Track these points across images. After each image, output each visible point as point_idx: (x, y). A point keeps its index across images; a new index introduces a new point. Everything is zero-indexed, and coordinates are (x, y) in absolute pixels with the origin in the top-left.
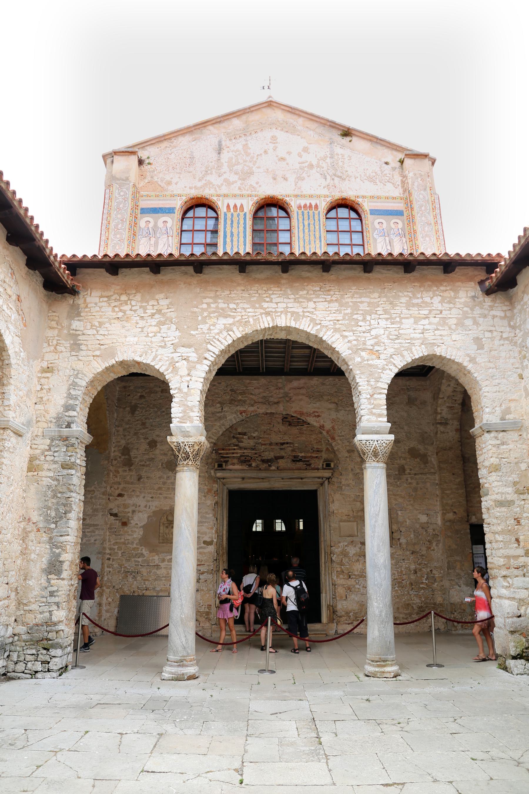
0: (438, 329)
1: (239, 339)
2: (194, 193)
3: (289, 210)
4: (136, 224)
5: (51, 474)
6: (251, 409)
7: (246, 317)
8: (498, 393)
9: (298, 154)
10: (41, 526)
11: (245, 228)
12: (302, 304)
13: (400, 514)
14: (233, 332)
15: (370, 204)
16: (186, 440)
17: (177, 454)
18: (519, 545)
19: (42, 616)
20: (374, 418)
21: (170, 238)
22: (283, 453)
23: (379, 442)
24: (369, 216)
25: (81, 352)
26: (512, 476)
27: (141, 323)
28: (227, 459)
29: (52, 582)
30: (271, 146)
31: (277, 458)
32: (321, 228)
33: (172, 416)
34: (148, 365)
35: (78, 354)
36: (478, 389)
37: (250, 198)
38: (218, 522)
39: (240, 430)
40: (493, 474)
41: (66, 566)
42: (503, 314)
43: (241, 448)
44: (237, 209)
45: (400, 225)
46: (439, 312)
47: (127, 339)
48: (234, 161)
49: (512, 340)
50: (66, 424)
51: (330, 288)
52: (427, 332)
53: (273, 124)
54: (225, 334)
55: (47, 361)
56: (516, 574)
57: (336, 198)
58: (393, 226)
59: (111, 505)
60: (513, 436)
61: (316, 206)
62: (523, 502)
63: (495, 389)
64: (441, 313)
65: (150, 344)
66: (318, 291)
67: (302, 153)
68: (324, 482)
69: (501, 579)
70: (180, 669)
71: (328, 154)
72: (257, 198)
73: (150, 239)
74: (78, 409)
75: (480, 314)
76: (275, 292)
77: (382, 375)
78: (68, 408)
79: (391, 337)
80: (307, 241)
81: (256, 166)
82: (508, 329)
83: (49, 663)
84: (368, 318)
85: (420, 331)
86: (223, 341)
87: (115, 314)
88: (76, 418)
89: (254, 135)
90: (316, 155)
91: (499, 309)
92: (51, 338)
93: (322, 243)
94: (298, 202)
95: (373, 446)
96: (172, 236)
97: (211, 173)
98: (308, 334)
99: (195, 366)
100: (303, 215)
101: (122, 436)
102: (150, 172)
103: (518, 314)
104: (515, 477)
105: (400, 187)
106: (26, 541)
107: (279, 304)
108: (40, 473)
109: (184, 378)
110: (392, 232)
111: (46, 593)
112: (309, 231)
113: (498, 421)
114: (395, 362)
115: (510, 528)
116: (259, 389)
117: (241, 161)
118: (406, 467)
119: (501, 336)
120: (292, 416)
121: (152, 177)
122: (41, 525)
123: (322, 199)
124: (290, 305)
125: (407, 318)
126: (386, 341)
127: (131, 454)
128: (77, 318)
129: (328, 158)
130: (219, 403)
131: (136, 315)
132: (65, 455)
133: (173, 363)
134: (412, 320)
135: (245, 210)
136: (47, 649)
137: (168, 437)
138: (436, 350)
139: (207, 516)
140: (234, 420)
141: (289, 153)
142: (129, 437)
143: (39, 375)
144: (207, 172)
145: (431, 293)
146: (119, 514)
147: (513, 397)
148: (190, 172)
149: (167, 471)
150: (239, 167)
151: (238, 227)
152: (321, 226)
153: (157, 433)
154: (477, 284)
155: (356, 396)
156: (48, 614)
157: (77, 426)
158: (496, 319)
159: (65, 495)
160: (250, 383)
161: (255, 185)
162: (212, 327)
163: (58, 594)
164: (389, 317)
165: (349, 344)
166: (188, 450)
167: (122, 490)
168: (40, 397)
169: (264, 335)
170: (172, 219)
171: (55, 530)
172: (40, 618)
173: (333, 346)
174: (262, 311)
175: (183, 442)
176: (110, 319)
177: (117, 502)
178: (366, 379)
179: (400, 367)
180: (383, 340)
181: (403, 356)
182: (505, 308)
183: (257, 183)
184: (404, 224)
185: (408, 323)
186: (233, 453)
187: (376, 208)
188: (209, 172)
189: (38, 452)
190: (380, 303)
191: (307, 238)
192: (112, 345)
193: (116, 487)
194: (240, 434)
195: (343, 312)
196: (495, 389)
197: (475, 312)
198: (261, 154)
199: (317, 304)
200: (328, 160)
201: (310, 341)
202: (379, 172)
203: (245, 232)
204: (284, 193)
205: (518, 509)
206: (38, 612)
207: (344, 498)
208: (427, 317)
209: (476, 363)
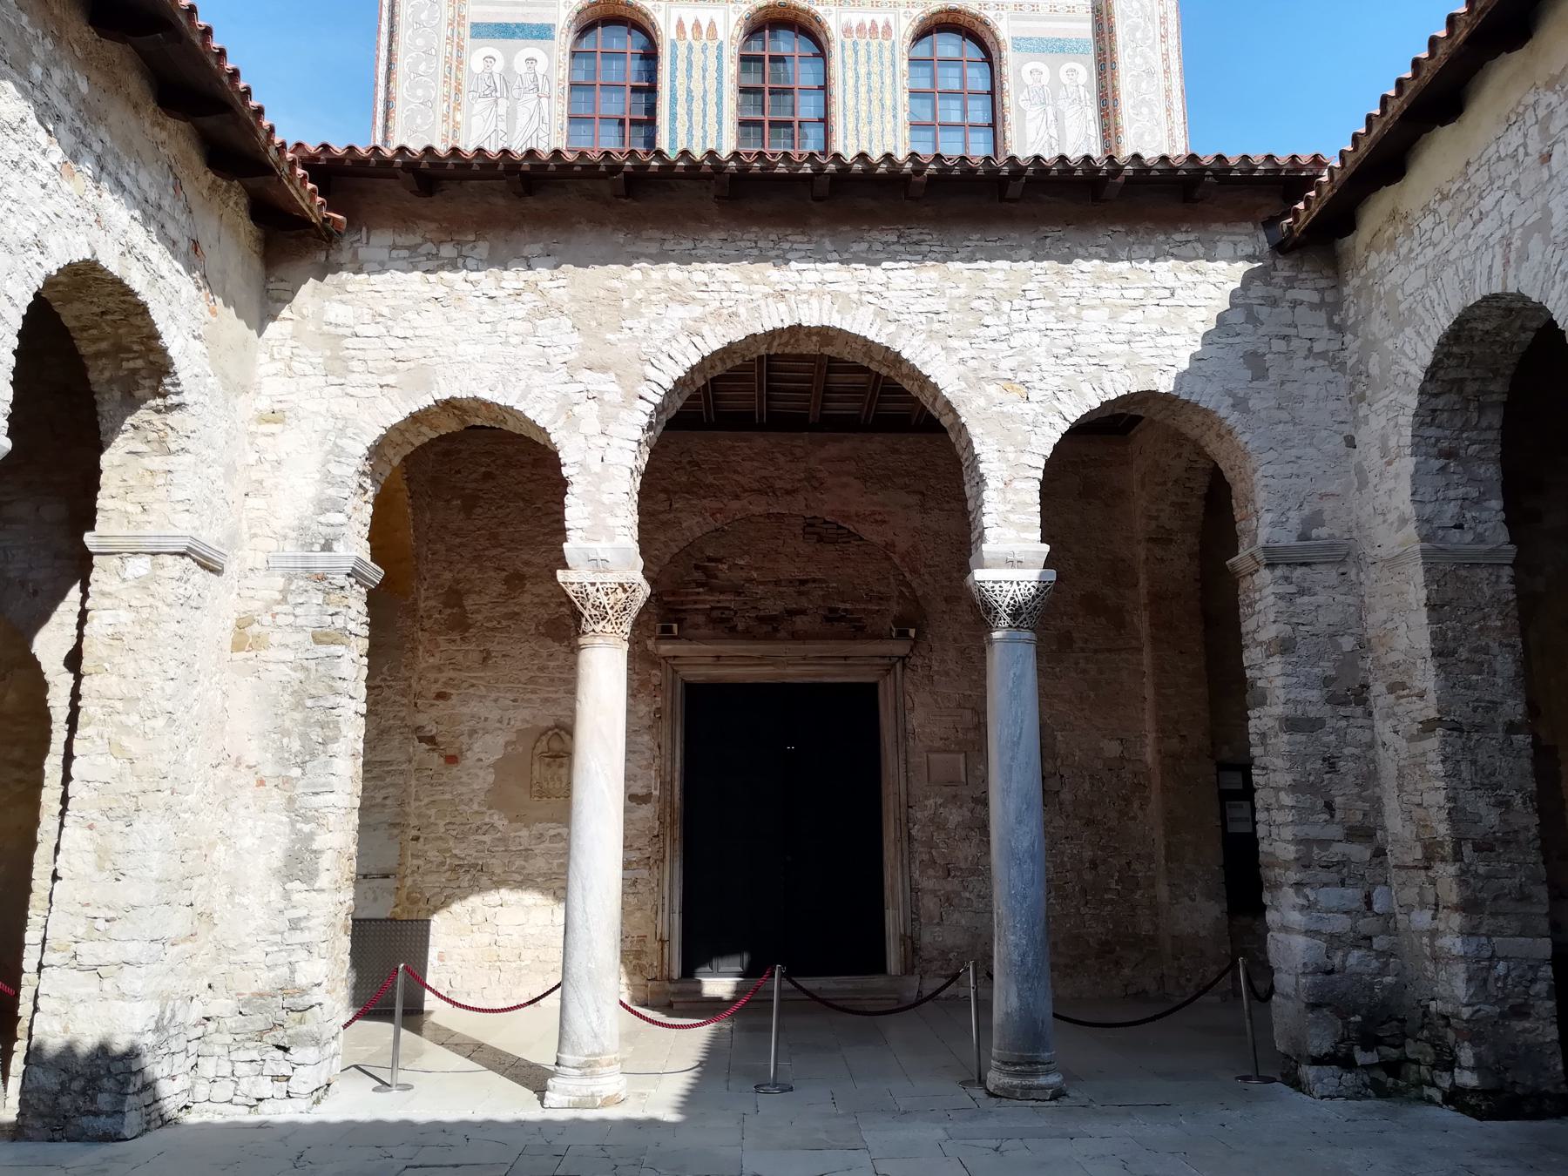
0: (1164, 333)
1: (714, 353)
3: (822, 38)
4: (462, 63)
5: (289, 655)
6: (735, 505)
7: (732, 303)
8: (1294, 480)
10: (268, 774)
11: (720, 82)
12: (856, 273)
13: (1060, 738)
14: (702, 337)
16: (598, 578)
17: (581, 609)
18: (1332, 816)
19: (272, 974)
20: (1011, 533)
21: (544, 101)
22: (804, 603)
23: (1022, 586)
25: (352, 377)
26: (1321, 664)
27: (491, 312)
28: (682, 615)
29: (296, 897)
31: (792, 613)
32: (898, 83)
33: (567, 525)
34: (509, 410)
35: (342, 381)
36: (1249, 471)
38: (663, 752)
39: (709, 552)
40: (1277, 659)
41: (325, 861)
42: (1315, 298)
43: (712, 590)
44: (701, 33)
46: (1167, 293)
47: (462, 346)
49: (1334, 358)
50: (323, 542)
51: (921, 237)
52: (1138, 339)
54: (684, 341)
55: (270, 396)
56: (1325, 880)
59: (421, 719)
60: (1326, 575)
61: (887, 26)
62: (1343, 723)
63: (1288, 469)
64: (1173, 295)
65: (513, 361)
66: (894, 243)
68: (894, 665)
69: (1291, 891)
70: (586, 1081)
72: (748, 6)
74: (349, 509)
75: (1263, 298)
76: (795, 246)
77: (1033, 438)
78: (325, 506)
79: (1055, 351)
80: (863, 115)
82: (1326, 332)
83: (288, 1079)
84: (1006, 306)
85: (1123, 338)
86: (679, 357)
87: (427, 288)
88: (343, 528)
91: (1309, 284)
92: (278, 343)
93: (899, 120)
94: (845, 18)
95: (1010, 595)
98: (867, 344)
99: (618, 413)
101: (444, 564)
103: (1351, 298)
104: (1326, 667)
106: (232, 807)
107: (804, 273)
108: (262, 653)
109: (594, 440)
110: (1062, 93)
111: (281, 923)
112: (869, 90)
113: (1293, 542)
114: (1061, 407)
115: (1312, 778)
116: (752, 460)
118: (1075, 635)
119: (1310, 349)
120: (826, 522)
122: (267, 770)
123: (902, 10)
124: (829, 277)
125: (1093, 307)
126: (1042, 361)
127: (465, 603)
128: (338, 297)
130: (665, 491)
131: (479, 294)
132: (322, 613)
133: (567, 408)
134: (1103, 313)
135: (720, 36)
136: (286, 1050)
137: (559, 572)
138: (1156, 380)
139: (639, 739)
140: (696, 529)
142: (460, 566)
143: (253, 428)
145: (1151, 248)
146: (439, 739)
147: (1332, 488)
149: (549, 642)
151: (704, 77)
152: (898, 79)
153: (526, 557)
154: (1260, 225)
155: (973, 483)
156: (285, 970)
157: (347, 547)
158: (1299, 309)
159: (322, 703)
160: (733, 447)
162: (653, 326)
163: (309, 924)
164: (1053, 304)
165: (961, 368)
166: (604, 600)
167: (446, 684)
168: (256, 481)
169: (769, 347)
170: (548, 53)
171: (301, 782)
172: (265, 980)
173: (925, 372)
174: (768, 290)
175: (593, 584)
176: (417, 302)
177: (434, 713)
178: (996, 447)
179: (1073, 420)
180: (1037, 359)
181: (1081, 395)
182: (1323, 283)
184: (1090, 74)
185: (1095, 318)
186: (695, 602)
187: (1027, 35)
189: (258, 605)
190: (1034, 271)
191: (863, 108)
192: (423, 361)
193: (432, 676)
194: (710, 559)
195: (948, 291)
196: (1288, 469)
197: (1250, 293)
199: (890, 274)
201: (872, 359)
203: (719, 91)
205: (1333, 737)
206: (262, 966)
207: (936, 701)
208: (1139, 305)
209: (1247, 410)
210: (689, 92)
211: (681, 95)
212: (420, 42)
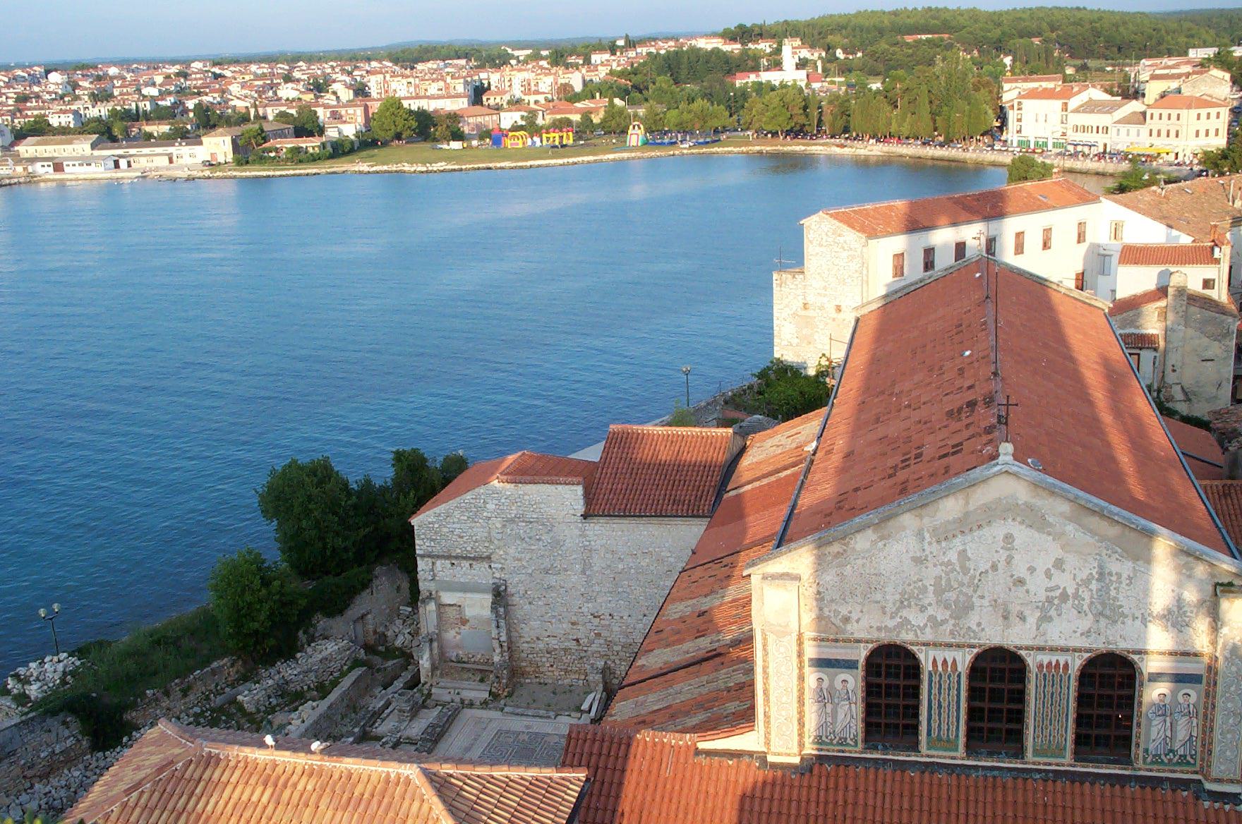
2: (885, 638)
48: (943, 583)
57: (1099, 652)
61: (1066, 666)
81: (979, 593)
90: (1075, 575)
96: (856, 704)
97: (909, 606)
100: (1045, 680)
123: (1077, 654)
129: (1094, 582)
135: (959, 669)
141: (1032, 570)
144: (902, 602)
161: (974, 627)
170: (855, 678)
184: (1198, 698)
188: (906, 603)
198: (987, 572)
200: (1094, 585)
204: (1018, 642)
212: (782, 684)
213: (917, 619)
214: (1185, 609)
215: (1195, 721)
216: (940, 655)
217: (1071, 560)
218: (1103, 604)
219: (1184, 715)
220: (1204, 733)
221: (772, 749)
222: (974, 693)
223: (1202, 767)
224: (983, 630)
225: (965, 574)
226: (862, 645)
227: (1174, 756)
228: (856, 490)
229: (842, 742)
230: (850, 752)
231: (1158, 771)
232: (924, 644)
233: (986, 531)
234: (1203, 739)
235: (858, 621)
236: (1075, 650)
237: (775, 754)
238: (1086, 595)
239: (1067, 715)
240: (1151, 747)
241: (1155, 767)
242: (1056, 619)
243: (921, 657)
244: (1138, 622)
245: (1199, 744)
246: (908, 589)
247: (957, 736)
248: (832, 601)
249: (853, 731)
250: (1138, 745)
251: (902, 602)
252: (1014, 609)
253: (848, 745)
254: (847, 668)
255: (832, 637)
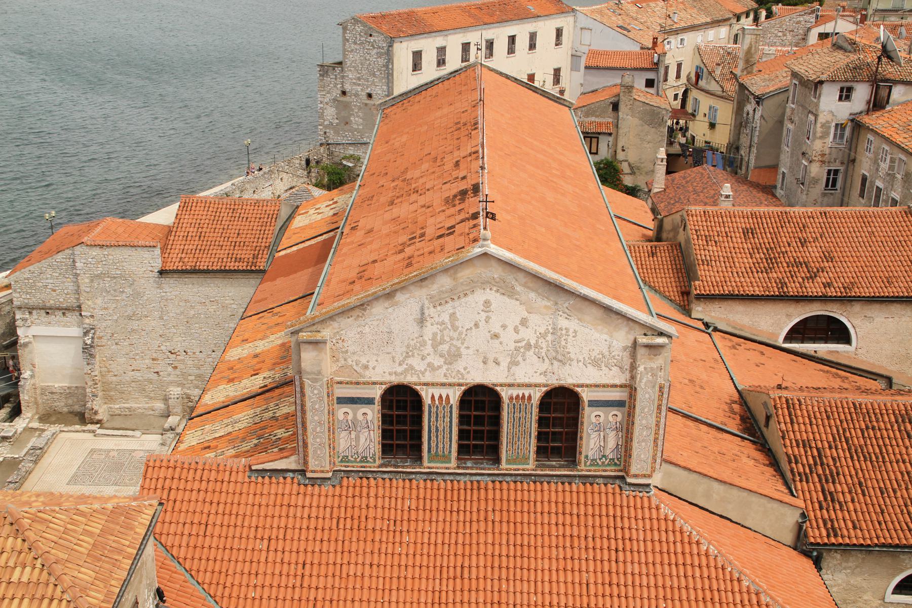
2: (395, 380)
9: (515, 329)
11: (451, 422)
15: (590, 394)
24: (587, 408)
30: (484, 315)
37: (457, 387)
45: (619, 419)
48: (439, 338)
53: (488, 282)
57: (553, 387)
58: (611, 419)
61: (530, 397)
67: (520, 326)
71: (550, 328)
73: (350, 433)
89: (463, 300)
97: (413, 356)
100: (514, 408)
102: (342, 352)
105: (628, 372)
117: (447, 339)
121: (345, 360)
123: (537, 388)
129: (550, 335)
144: (407, 353)
148: (388, 353)
150: (445, 348)
151: (444, 421)
161: (462, 371)
170: (373, 411)
183: (465, 369)
184: (623, 417)
188: (410, 354)
198: (471, 328)
200: (550, 337)
202: (607, 353)
204: (495, 381)
210: (437, 428)
211: (433, 429)
212: (316, 418)
213: (419, 365)
214: (613, 354)
215: (620, 434)
216: (437, 392)
217: (534, 319)
218: (557, 352)
219: (613, 430)
220: (626, 442)
221: (310, 468)
222: (463, 419)
223: (625, 466)
224: (468, 372)
225: (455, 331)
226: (378, 386)
227: (606, 459)
228: (375, 261)
229: (364, 459)
230: (370, 467)
231: (595, 471)
232: (425, 384)
233: (470, 298)
234: (626, 446)
235: (374, 369)
236: (536, 386)
237: (312, 471)
238: (544, 345)
239: (530, 433)
240: (590, 454)
241: (593, 468)
242: (522, 363)
243: (423, 394)
244: (581, 364)
245: (623, 449)
246: (412, 343)
247: (450, 452)
248: (354, 353)
249: (372, 451)
250: (580, 453)
251: (407, 353)
252: (491, 357)
253: (368, 462)
254: (366, 404)
255: (354, 380)
